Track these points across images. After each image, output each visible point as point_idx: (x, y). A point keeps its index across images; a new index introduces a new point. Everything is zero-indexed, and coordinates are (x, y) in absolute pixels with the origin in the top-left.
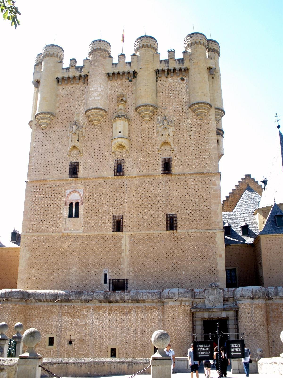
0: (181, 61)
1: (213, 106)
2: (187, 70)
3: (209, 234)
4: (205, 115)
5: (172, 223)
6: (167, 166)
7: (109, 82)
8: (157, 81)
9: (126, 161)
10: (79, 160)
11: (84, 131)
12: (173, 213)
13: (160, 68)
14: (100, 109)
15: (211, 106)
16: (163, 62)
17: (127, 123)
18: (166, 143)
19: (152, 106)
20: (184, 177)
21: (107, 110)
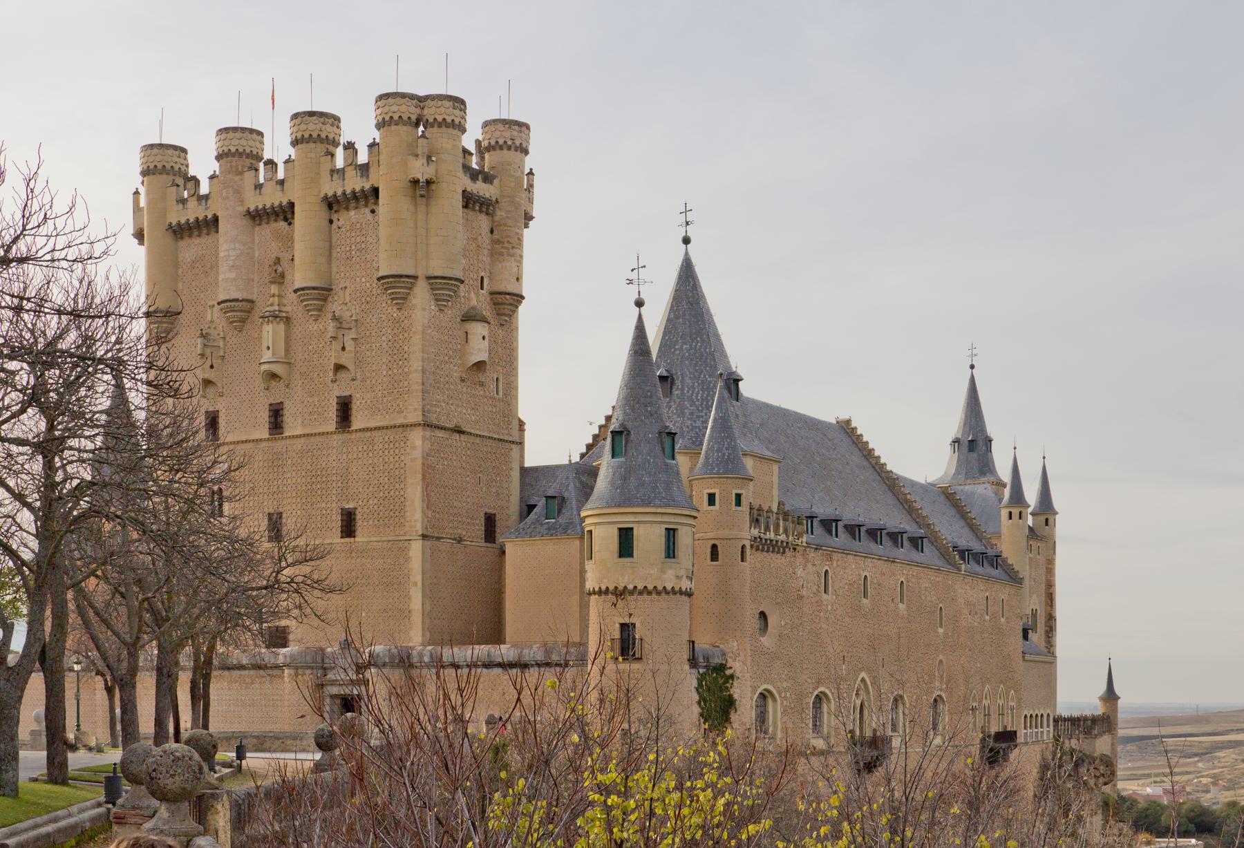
0: (364, 169)
1: (419, 273)
2: (376, 191)
3: (401, 544)
4: (405, 299)
5: (348, 526)
6: (344, 410)
7: (257, 228)
8: (331, 222)
9: (286, 405)
10: (219, 407)
11: (221, 344)
12: (351, 505)
13: (330, 194)
14: (237, 300)
15: (415, 278)
16: (335, 176)
17: (282, 326)
18: (339, 368)
19: (314, 288)
20: (369, 434)
21: (254, 297)
